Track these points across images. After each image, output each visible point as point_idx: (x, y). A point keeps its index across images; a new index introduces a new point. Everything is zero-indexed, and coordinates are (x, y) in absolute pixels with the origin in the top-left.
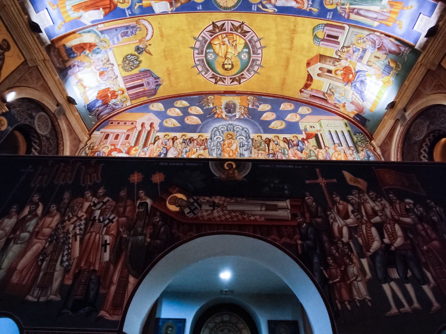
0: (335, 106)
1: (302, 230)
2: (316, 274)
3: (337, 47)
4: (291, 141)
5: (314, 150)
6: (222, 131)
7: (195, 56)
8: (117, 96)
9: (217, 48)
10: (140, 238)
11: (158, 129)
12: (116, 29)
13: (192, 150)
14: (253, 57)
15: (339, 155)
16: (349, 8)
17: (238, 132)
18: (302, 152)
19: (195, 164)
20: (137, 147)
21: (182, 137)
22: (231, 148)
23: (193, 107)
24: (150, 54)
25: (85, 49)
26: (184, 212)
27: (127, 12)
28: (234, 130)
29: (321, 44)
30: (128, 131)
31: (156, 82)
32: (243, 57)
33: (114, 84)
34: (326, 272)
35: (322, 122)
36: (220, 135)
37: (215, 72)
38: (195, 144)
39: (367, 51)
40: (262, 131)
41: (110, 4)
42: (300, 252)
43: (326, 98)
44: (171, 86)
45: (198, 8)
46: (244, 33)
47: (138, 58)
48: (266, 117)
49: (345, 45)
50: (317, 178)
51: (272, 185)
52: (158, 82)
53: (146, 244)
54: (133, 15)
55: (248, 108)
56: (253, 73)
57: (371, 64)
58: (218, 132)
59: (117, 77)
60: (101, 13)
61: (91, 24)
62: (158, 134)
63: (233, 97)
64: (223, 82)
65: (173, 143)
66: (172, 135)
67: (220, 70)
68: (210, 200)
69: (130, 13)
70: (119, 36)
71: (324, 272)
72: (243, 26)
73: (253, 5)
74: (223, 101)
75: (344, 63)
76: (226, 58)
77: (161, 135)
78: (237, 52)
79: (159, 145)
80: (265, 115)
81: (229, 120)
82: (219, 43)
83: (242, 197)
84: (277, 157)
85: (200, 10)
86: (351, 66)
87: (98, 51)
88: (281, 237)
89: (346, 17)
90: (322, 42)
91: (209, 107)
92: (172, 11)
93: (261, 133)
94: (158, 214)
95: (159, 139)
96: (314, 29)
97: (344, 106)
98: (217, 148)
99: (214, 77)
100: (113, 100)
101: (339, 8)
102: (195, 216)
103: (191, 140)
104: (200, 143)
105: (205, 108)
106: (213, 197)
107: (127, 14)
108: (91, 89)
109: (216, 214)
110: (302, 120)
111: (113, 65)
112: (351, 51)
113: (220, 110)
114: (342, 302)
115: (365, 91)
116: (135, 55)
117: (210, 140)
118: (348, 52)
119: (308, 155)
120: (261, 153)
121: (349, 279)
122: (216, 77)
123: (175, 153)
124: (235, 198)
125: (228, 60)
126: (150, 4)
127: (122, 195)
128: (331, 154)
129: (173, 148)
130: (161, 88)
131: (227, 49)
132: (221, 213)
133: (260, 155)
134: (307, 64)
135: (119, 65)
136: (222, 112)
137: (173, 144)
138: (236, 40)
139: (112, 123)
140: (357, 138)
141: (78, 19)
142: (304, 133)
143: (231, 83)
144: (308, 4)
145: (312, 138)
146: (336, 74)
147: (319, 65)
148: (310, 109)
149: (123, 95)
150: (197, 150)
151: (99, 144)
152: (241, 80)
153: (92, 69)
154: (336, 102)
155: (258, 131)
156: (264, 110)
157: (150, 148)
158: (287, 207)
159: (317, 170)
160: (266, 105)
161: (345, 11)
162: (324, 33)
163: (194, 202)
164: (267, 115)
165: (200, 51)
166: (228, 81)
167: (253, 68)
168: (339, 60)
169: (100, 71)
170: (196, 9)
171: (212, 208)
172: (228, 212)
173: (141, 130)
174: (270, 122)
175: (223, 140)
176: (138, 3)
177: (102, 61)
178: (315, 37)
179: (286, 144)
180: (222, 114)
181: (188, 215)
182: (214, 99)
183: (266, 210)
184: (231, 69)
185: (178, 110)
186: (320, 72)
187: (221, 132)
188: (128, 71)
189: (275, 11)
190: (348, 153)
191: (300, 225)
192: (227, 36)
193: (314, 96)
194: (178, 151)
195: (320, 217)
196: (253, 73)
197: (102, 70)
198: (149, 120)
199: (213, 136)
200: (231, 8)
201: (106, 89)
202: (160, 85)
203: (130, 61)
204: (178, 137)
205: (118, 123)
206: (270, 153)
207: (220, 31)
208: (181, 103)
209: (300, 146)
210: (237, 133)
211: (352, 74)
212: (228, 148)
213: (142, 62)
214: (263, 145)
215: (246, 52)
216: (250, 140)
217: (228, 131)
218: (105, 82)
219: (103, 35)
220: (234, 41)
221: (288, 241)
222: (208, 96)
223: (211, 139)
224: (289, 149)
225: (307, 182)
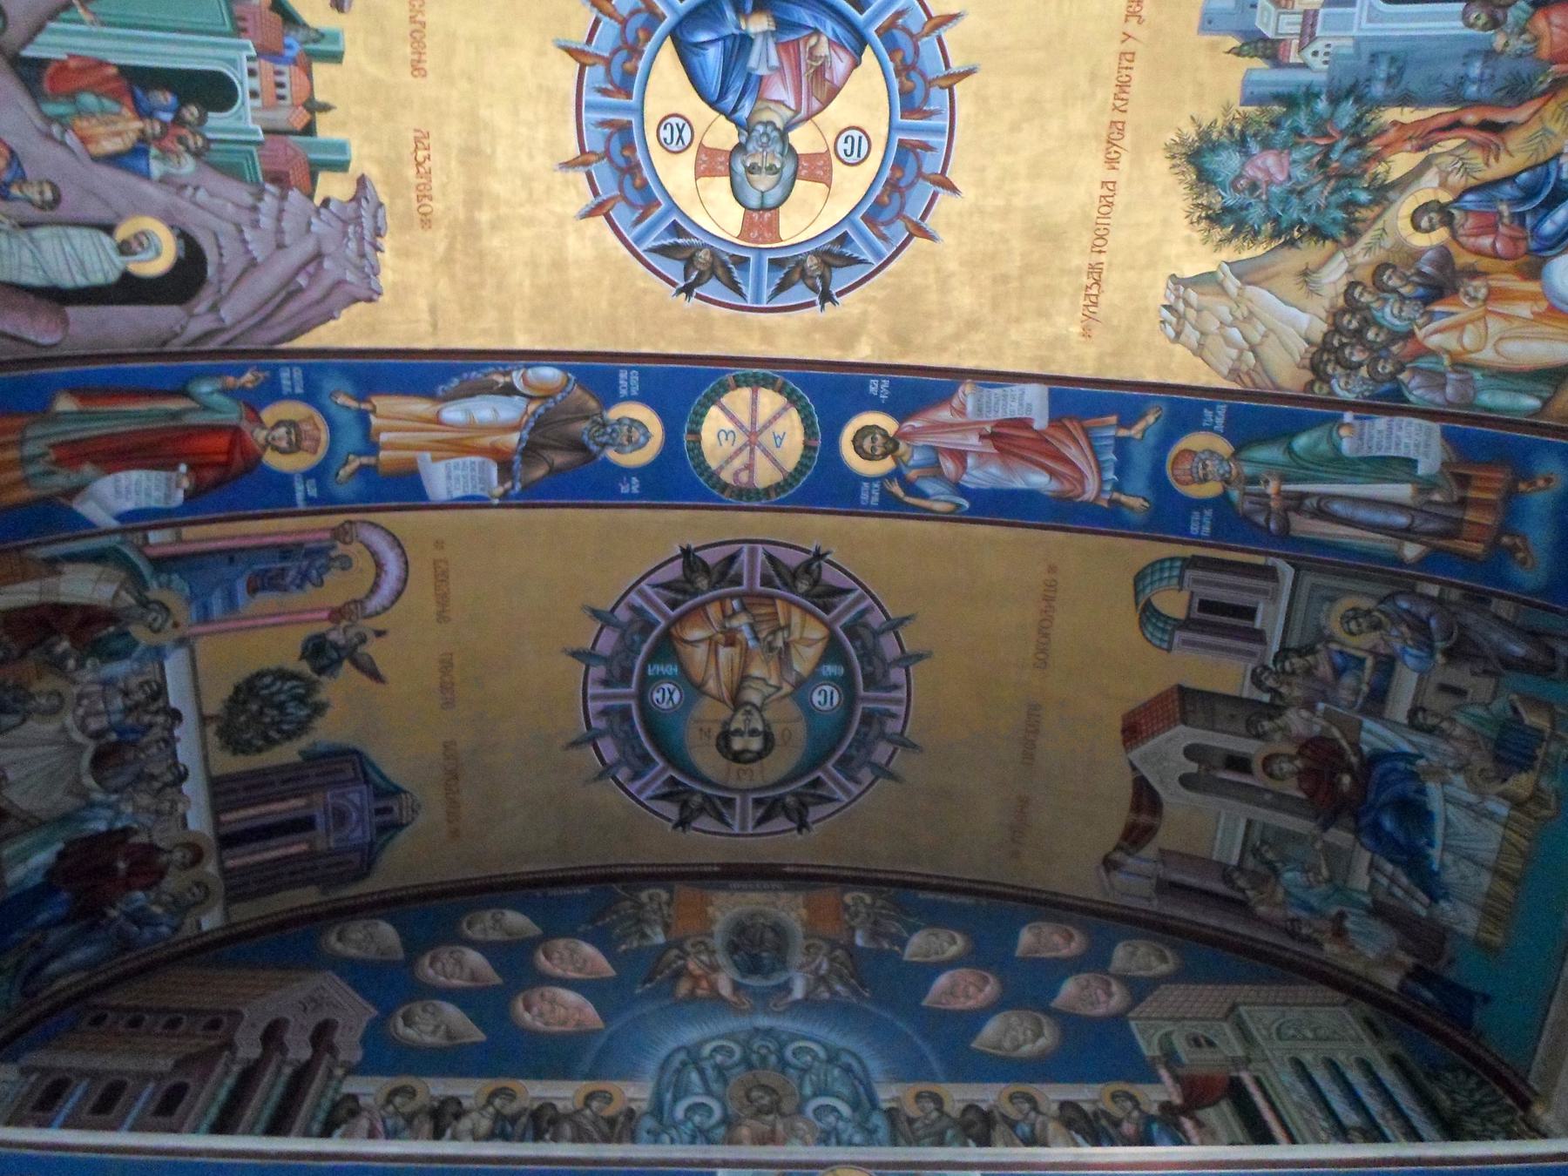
0: (1293, 935)
3: (1252, 654)
4: (1104, 1122)
6: (721, 1070)
7: (590, 691)
8: (162, 874)
9: (698, 656)
11: (357, 1056)
12: (230, 555)
14: (869, 699)
16: (1279, 493)
17: (804, 1071)
21: (489, 1102)
23: (561, 943)
24: (375, 675)
25: (55, 632)
27: (299, 488)
28: (783, 1064)
29: (1176, 641)
30: (177, 1065)
31: (379, 812)
32: (817, 698)
33: (158, 813)
35: (1245, 1016)
36: (709, 1092)
37: (682, 770)
39: (1399, 666)
40: (936, 1066)
41: (229, 452)
43: (1239, 896)
44: (455, 834)
45: (624, 489)
46: (825, 597)
47: (311, 687)
48: (951, 992)
49: (1293, 643)
52: (388, 810)
54: (324, 503)
55: (850, 949)
56: (866, 775)
57: (1431, 721)
58: (694, 1076)
59: (182, 777)
60: (178, 486)
61: (114, 524)
62: (353, 1086)
63: (772, 896)
64: (720, 818)
67: (707, 760)
69: (313, 492)
70: (241, 586)
72: (819, 567)
73: (866, 485)
74: (718, 914)
75: (1297, 721)
76: (737, 702)
78: (792, 678)
80: (943, 981)
81: (753, 1011)
82: (710, 638)
85: (631, 496)
86: (1336, 733)
87: (118, 645)
89: (1273, 526)
90: (1179, 635)
91: (646, 943)
92: (505, 495)
93: (931, 1077)
96: (1139, 578)
97: (1340, 933)
99: (673, 793)
100: (139, 895)
101: (1235, 494)
105: (623, 947)
107: (299, 496)
108: (32, 827)
110: (1148, 1007)
111: (176, 716)
112: (1324, 670)
113: (704, 958)
115: (1431, 852)
116: (294, 676)
117: (649, 1123)
118: (1309, 672)
122: (685, 797)
125: (749, 712)
126: (413, 461)
130: (403, 836)
131: (745, 665)
134: (1123, 731)
135: (204, 720)
136: (715, 968)
138: (788, 626)
139: (97, 1021)
140: (1450, 1093)
141: (62, 500)
142: (1164, 1073)
143: (760, 821)
144: (1102, 482)
146: (1271, 775)
147: (1183, 735)
148: (1168, 953)
149: (193, 873)
152: (811, 809)
153: (64, 730)
154: (1292, 913)
155: (911, 1069)
156: (933, 958)
160: (944, 935)
161: (1267, 506)
162: (1185, 595)
164: (954, 985)
165: (617, 672)
166: (743, 815)
167: (869, 753)
168: (1274, 710)
169: (103, 741)
170: (616, 493)
173: (258, 1062)
174: (975, 1019)
176: (359, 454)
177: (126, 693)
178: (1149, 614)
180: (714, 976)
182: (669, 904)
184: (760, 755)
185: (474, 958)
186: (1193, 767)
187: (710, 1073)
188: (243, 752)
189: (959, 506)
192: (744, 608)
193: (1175, 886)
196: (866, 775)
197: (113, 737)
199: (668, 1096)
200: (767, 491)
201: (110, 833)
202: (398, 826)
203: (268, 702)
204: (466, 1103)
205: (135, 1023)
207: (713, 587)
208: (497, 921)
210: (801, 1079)
211: (1349, 769)
213: (329, 713)
215: (832, 679)
217: (750, 1066)
218: (114, 797)
219: (164, 578)
220: (782, 629)
222: (641, 889)
223: (658, 1110)
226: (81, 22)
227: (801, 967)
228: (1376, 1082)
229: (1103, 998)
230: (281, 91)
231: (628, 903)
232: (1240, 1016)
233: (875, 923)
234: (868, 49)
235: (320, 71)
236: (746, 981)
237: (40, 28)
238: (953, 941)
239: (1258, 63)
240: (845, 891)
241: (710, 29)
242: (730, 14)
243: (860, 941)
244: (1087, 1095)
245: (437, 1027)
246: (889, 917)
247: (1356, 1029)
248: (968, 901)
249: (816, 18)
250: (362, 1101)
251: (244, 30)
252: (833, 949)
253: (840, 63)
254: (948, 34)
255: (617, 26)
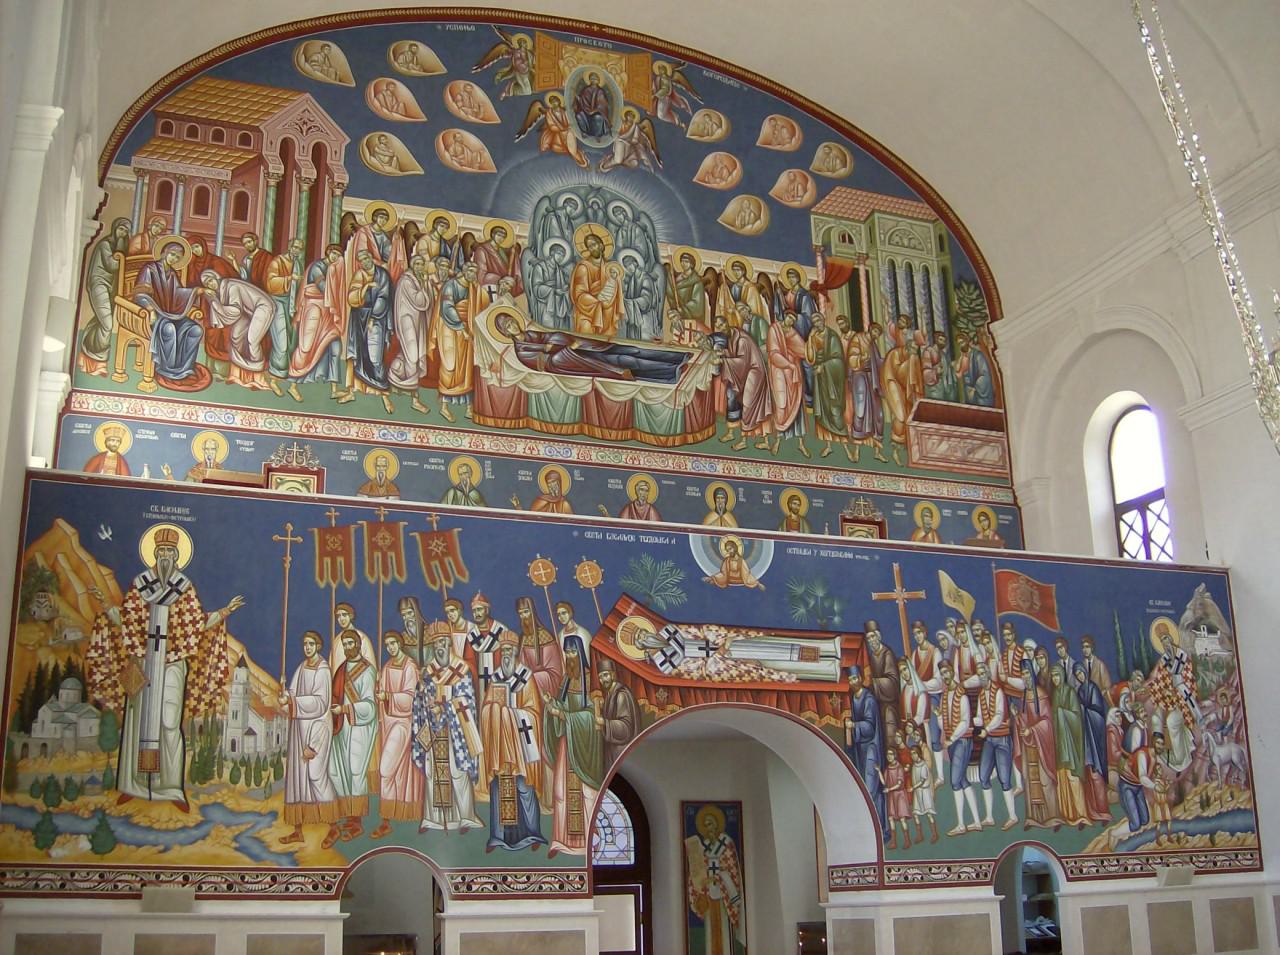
1: (855, 700)
2: (869, 778)
5: (840, 333)
6: (569, 218)
10: (584, 715)
13: (475, 289)
15: (903, 359)
17: (620, 227)
18: (806, 339)
19: (661, 540)
20: (285, 258)
21: (434, 229)
22: (601, 298)
23: (461, 84)
26: (652, 661)
28: (607, 221)
34: (883, 773)
35: (876, 221)
36: (563, 237)
38: (484, 267)
40: (695, 235)
42: (849, 742)
50: (891, 588)
51: (812, 603)
53: (597, 727)
55: (653, 119)
58: (554, 222)
65: (409, 251)
66: (402, 213)
68: (699, 634)
71: (880, 773)
77: (360, 207)
79: (362, 256)
81: (587, 170)
83: (758, 629)
84: (734, 347)
88: (821, 713)
91: (519, 93)
94: (606, 664)
95: (355, 228)
98: (555, 293)
102: (676, 671)
103: (467, 246)
104: (500, 262)
106: (705, 627)
109: (712, 669)
114: (897, 820)
117: (529, 256)
119: (821, 351)
120: (690, 330)
121: (912, 786)
123: (420, 295)
124: (744, 632)
127: (525, 619)
128: (883, 356)
129: (409, 273)
132: (722, 666)
133: (687, 333)
136: (566, 126)
137: (409, 259)
139: (167, 128)
140: (960, 299)
142: (819, 260)
145: (840, 286)
150: (490, 292)
151: (147, 229)
155: (680, 237)
157: (331, 268)
158: (834, 654)
159: (896, 566)
163: (669, 639)
171: (703, 654)
172: (733, 663)
174: (723, 198)
175: (573, 260)
179: (763, 299)
181: (662, 669)
183: (801, 658)
187: (563, 219)
190: (927, 355)
191: (852, 692)
194: (428, 291)
195: (886, 676)
198: (305, 128)
206: (716, 330)
209: (804, 315)
212: (589, 297)
214: (698, 298)
216: (658, 271)
221: (833, 721)
222: (513, 33)
223: (533, 247)
224: (773, 321)
225: (875, 596)
227: (621, 133)
228: (927, 285)
229: (800, 193)
231: (503, 47)
232: (873, 222)
233: (672, 96)
236: (585, 142)
238: (720, 126)
240: (656, 59)
243: (660, 115)
244: (775, 269)
245: (391, 158)
246: (681, 92)
247: (933, 244)
248: (734, 83)
250: (358, 217)
252: (642, 120)
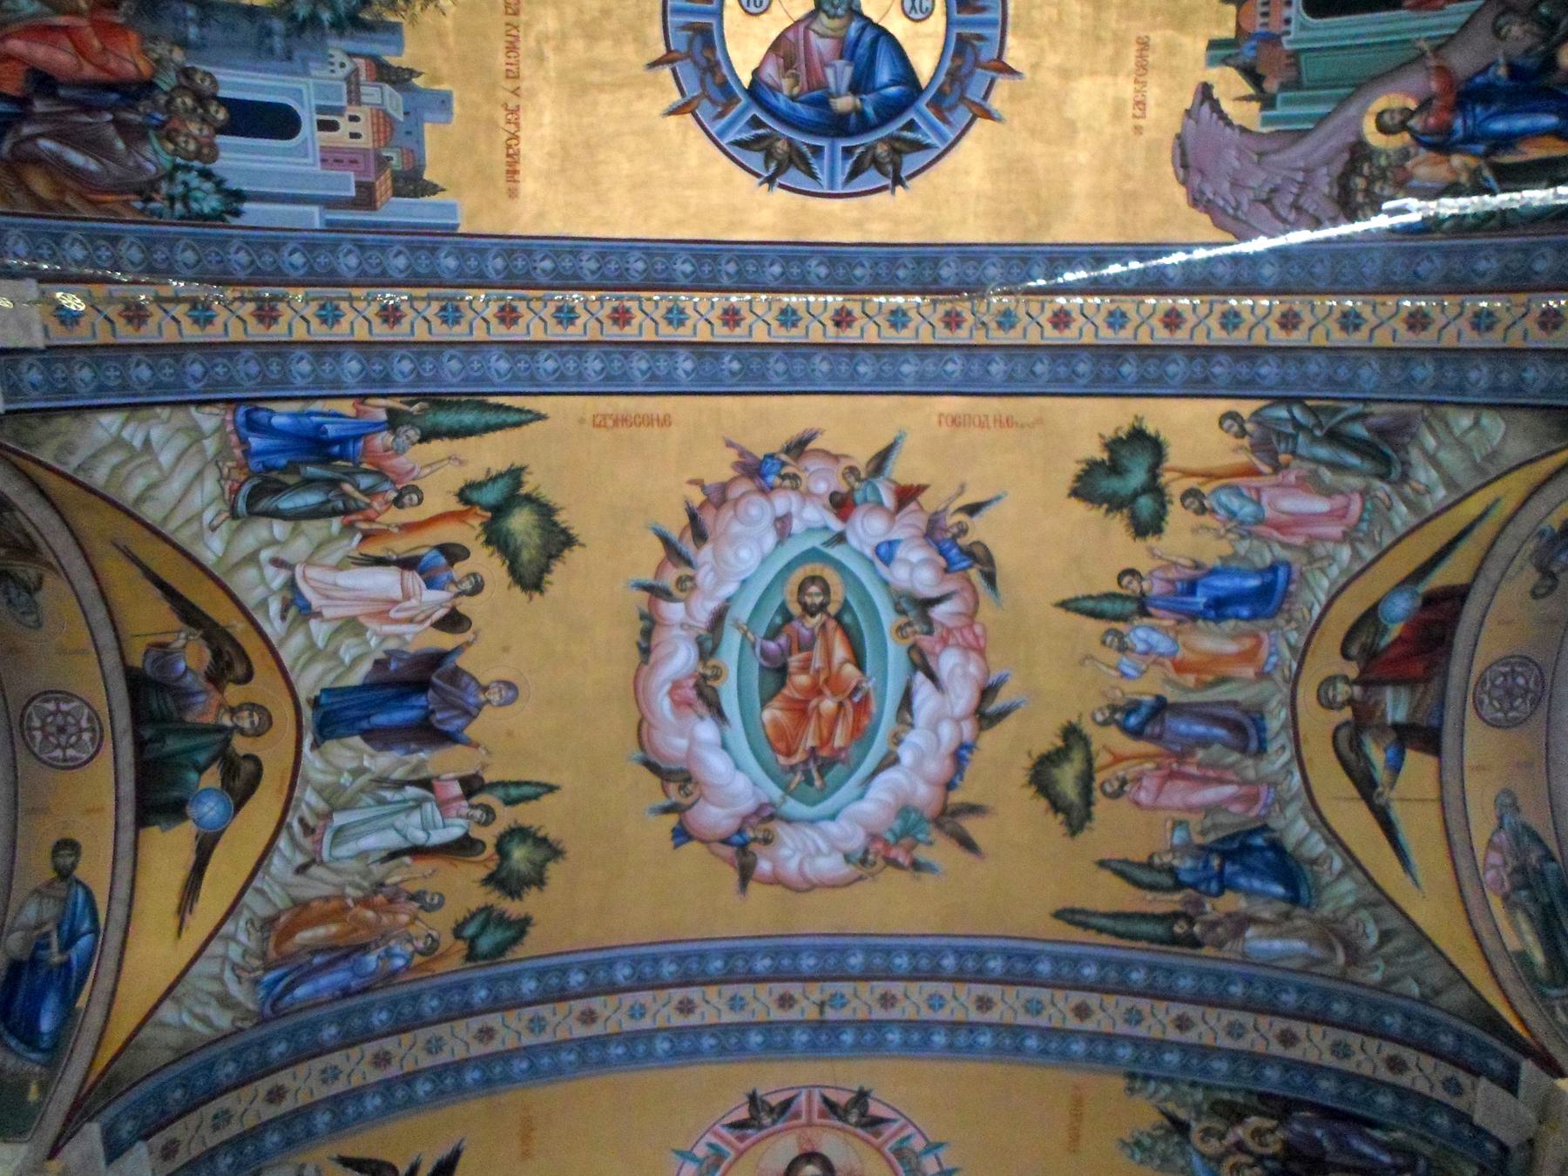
226: (1429, 39)
230: (1264, 9)
234: (746, 86)
235: (1227, 31)
237: (1464, 27)
239: (394, 61)
241: (887, 98)
242: (869, 110)
249: (794, 109)
251: (1289, 56)
253: (771, 73)
254: (676, 97)
255: (968, 95)
